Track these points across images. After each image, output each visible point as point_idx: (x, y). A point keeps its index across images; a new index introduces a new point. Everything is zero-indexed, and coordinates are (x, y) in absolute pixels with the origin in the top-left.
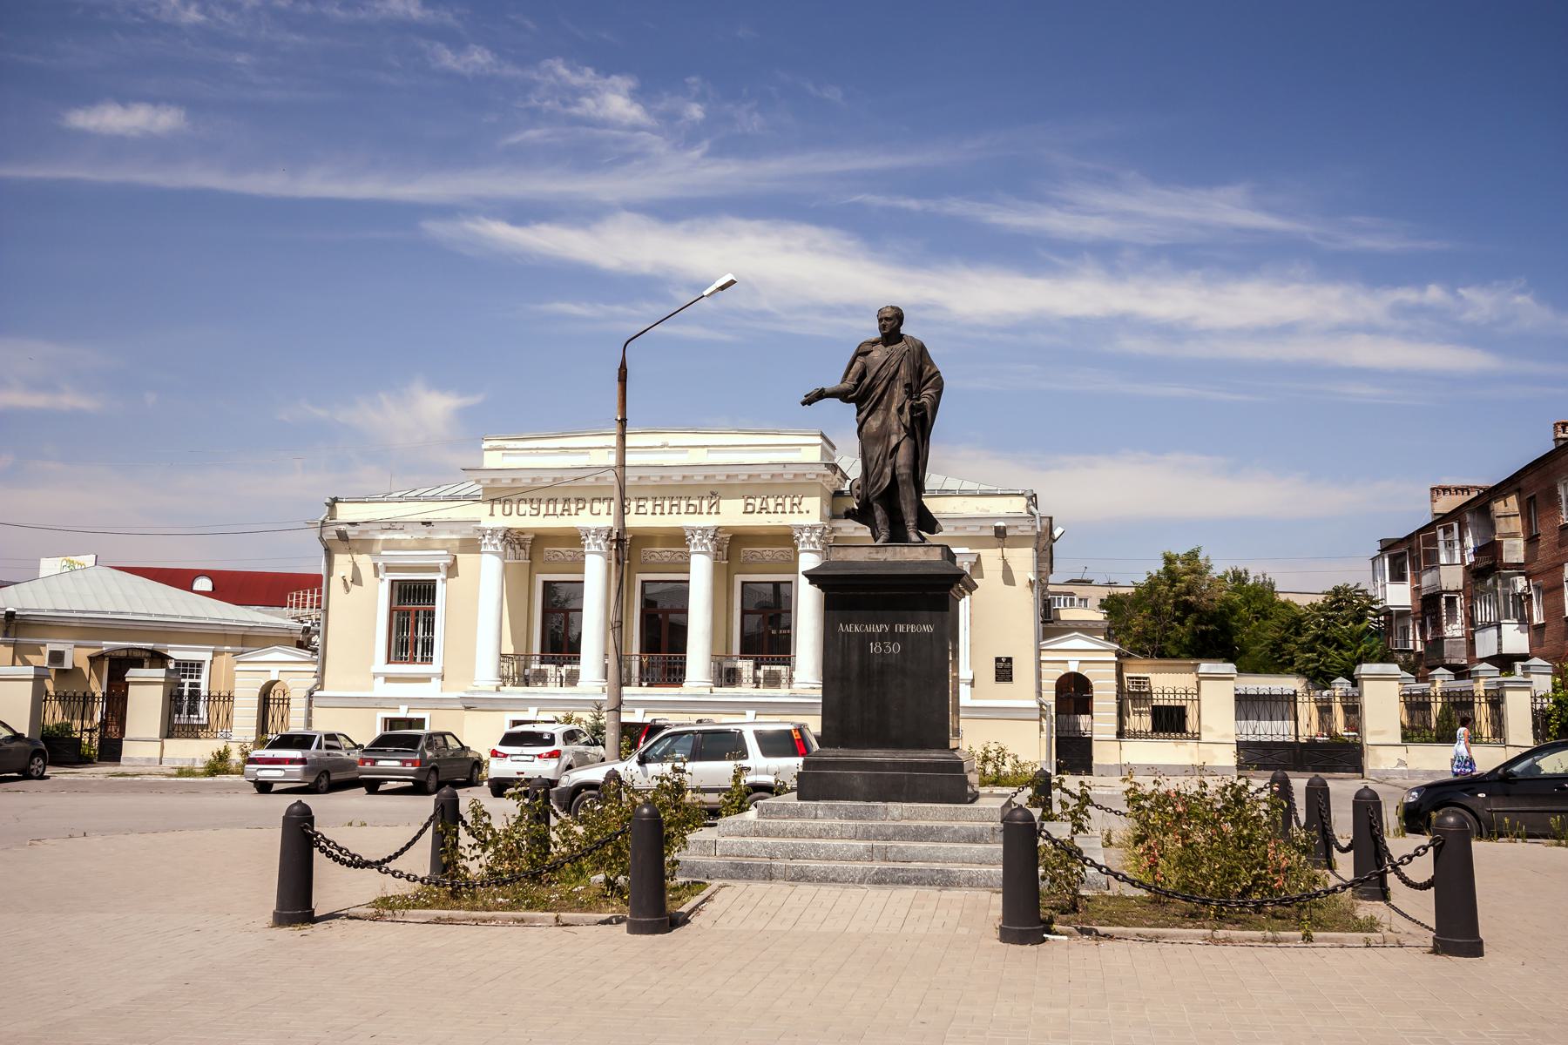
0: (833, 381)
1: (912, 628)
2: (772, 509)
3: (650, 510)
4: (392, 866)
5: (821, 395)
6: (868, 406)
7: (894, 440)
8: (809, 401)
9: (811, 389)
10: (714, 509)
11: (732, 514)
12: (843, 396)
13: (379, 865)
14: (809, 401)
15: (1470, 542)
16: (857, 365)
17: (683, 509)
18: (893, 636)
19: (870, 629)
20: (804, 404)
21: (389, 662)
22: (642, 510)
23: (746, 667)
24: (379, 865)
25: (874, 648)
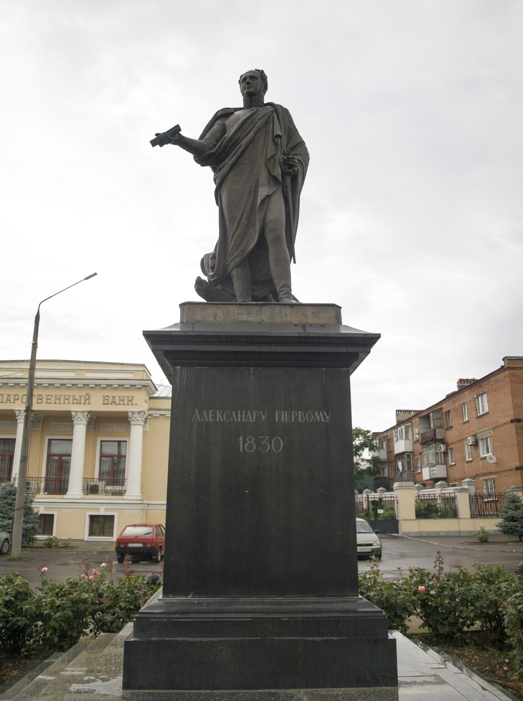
1: (300, 416)
2: (117, 402)
3: (53, 402)
5: (172, 137)
6: (230, 161)
7: (263, 192)
8: (160, 140)
9: (164, 129)
10: (87, 402)
11: (97, 404)
14: (160, 140)
15: (416, 430)
16: (216, 127)
17: (71, 402)
19: (239, 417)
20: (154, 143)
22: (49, 401)
23: (101, 485)
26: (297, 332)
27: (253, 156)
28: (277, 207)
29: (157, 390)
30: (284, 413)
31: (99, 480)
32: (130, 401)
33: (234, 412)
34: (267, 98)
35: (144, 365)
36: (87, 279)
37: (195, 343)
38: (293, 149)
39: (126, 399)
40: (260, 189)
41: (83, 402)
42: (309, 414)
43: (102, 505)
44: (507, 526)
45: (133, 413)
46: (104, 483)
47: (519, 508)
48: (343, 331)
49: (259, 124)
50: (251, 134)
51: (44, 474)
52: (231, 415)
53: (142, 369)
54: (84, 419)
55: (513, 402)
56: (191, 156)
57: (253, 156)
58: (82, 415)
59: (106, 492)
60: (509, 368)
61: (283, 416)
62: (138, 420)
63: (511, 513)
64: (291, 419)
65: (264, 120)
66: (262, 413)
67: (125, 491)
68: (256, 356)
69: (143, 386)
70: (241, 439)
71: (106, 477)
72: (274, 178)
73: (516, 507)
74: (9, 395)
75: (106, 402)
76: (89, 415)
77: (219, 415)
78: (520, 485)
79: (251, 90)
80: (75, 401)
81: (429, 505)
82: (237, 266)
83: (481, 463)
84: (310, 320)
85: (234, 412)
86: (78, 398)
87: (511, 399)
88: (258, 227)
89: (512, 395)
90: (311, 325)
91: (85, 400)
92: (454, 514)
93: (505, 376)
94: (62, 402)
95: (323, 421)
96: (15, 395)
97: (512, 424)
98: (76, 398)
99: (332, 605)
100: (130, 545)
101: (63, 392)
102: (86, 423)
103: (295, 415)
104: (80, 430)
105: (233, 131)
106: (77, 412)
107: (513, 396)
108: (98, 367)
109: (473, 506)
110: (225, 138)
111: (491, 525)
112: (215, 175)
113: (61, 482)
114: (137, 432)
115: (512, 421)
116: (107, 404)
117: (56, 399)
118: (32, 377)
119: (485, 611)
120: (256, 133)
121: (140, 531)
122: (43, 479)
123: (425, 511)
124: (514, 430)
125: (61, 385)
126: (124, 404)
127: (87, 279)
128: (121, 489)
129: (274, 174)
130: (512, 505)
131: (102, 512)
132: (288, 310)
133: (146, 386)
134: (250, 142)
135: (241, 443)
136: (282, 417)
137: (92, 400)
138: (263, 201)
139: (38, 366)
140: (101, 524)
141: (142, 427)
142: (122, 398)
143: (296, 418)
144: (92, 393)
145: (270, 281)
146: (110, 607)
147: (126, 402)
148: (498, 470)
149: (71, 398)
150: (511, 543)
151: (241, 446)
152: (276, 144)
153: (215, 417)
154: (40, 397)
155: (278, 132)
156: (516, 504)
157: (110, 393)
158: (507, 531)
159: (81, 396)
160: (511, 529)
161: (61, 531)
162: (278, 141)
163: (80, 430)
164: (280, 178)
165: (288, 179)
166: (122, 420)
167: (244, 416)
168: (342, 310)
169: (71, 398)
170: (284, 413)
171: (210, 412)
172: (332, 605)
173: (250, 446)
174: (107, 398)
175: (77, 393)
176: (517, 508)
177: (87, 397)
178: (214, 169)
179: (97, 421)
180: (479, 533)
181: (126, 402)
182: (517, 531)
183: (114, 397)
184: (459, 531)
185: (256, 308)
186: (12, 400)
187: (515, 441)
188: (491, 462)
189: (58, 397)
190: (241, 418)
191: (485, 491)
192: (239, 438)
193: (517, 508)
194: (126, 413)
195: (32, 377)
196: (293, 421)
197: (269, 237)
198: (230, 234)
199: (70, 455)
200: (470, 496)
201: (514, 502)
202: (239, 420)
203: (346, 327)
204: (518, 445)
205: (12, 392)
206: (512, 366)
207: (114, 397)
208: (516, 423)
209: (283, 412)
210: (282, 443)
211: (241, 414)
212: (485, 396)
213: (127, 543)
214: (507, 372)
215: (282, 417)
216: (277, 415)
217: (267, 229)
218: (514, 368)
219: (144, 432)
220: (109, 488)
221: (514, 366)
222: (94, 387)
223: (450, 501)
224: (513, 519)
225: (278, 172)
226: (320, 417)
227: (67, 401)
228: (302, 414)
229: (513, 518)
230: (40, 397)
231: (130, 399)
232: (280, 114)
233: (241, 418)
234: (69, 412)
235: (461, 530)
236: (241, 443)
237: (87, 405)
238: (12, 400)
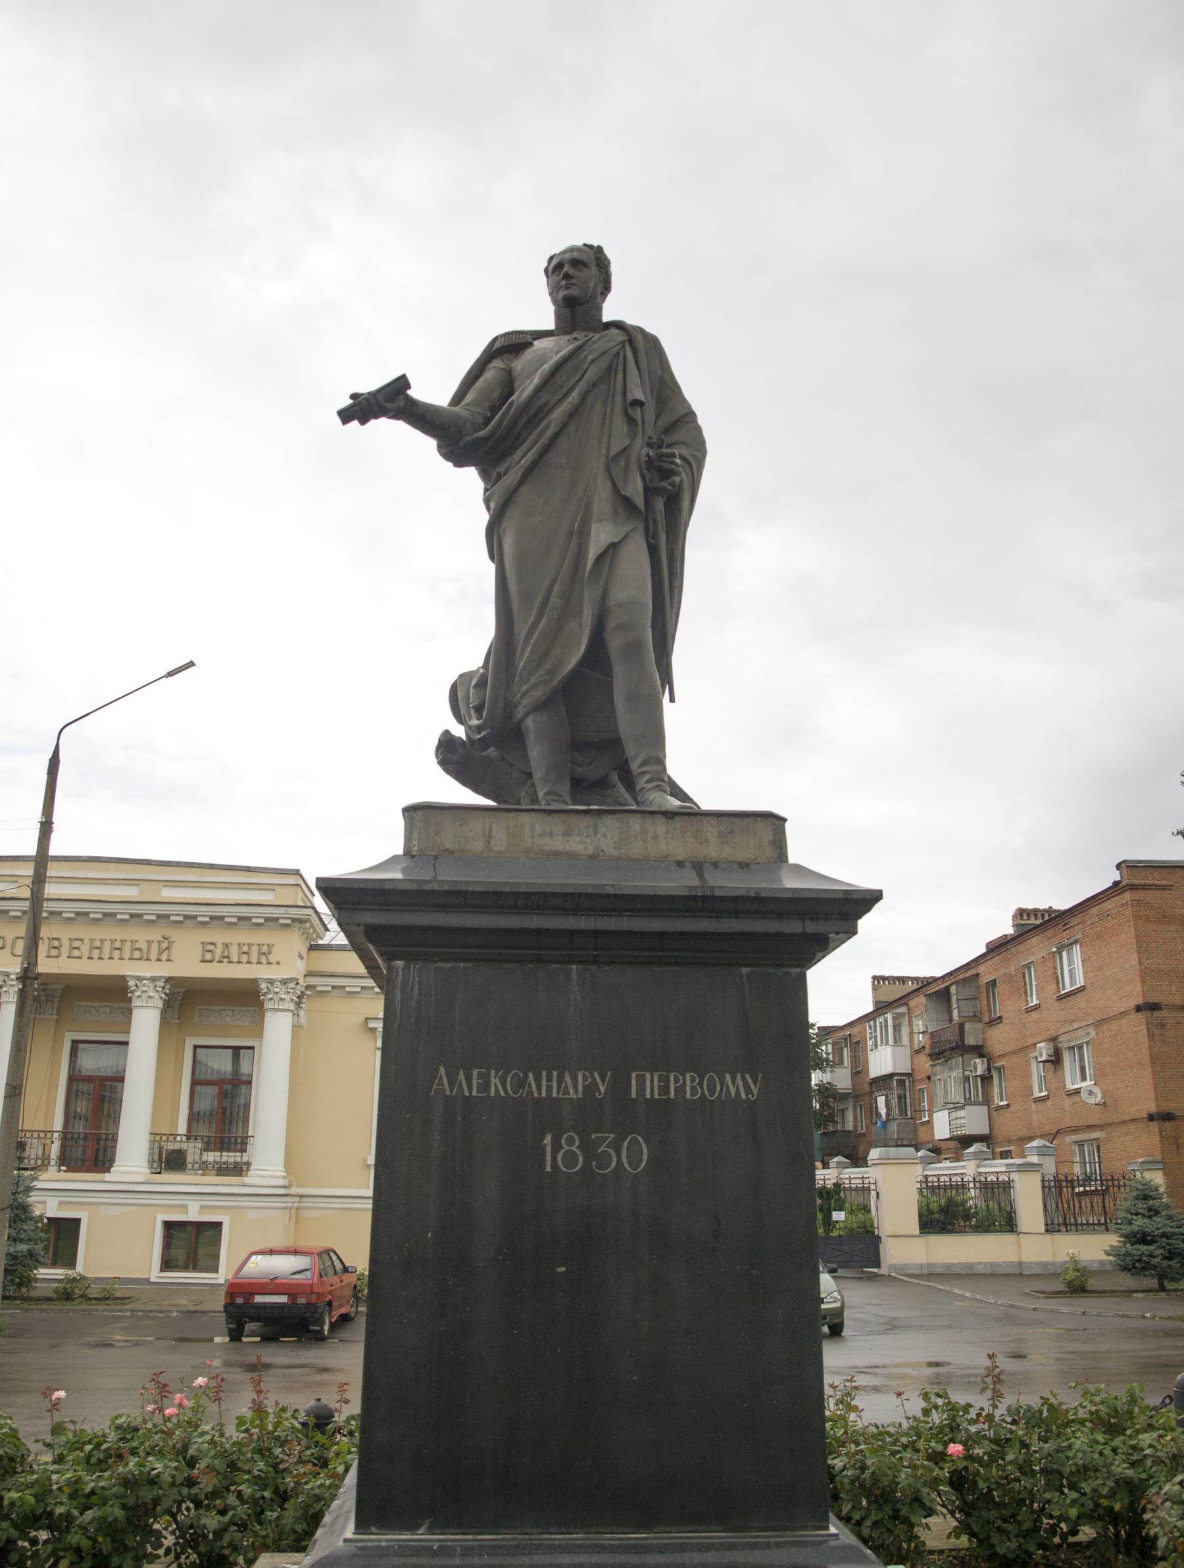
1: (689, 1085)
2: (235, 958)
3: (86, 955)
5: (390, 401)
6: (522, 458)
7: (601, 535)
8: (361, 409)
9: (370, 384)
10: (164, 956)
11: (188, 962)
14: (361, 409)
15: (919, 1025)
16: (489, 375)
17: (127, 955)
18: (624, 1114)
19: (543, 1087)
20: (346, 416)
22: (76, 953)
23: (193, 1150)
25: (560, 1154)
26: (680, 883)
27: (576, 441)
29: (327, 930)
30: (652, 1077)
31: (188, 1138)
32: (265, 954)
33: (531, 1075)
34: (611, 310)
35: (297, 873)
36: (170, 674)
37: (441, 908)
38: (667, 431)
39: (255, 949)
40: (595, 529)
41: (154, 955)
42: (711, 1079)
43: (193, 1196)
44: (1131, 1255)
45: (271, 982)
46: (199, 1145)
47: (1157, 1213)
48: (791, 883)
49: (593, 372)
50: (574, 396)
51: (58, 1125)
52: (521, 1083)
53: (292, 880)
54: (157, 996)
55: (1140, 964)
56: (429, 444)
57: (576, 441)
58: (152, 985)
59: (204, 1167)
60: (1132, 887)
61: (648, 1084)
62: (282, 999)
63: (1139, 1223)
64: (667, 1092)
65: (603, 363)
66: (597, 1078)
67: (248, 1164)
68: (585, 946)
69: (294, 920)
70: (548, 1140)
71: (203, 1130)
72: (628, 502)
73: (1150, 1209)
75: (208, 956)
76: (168, 986)
77: (495, 1081)
78: (1158, 1157)
79: (574, 292)
80: (137, 954)
81: (950, 1201)
82: (538, 708)
83: (1067, 1102)
84: (713, 850)
85: (531, 1075)
86: (144, 946)
87: (1135, 957)
88: (588, 618)
89: (1139, 948)
90: (715, 864)
91: (160, 952)
92: (1008, 1224)
93: (1123, 905)
94: (106, 954)
95: (743, 1096)
97: (1139, 1015)
98: (138, 945)
100: (259, 1299)
101: (107, 933)
102: (160, 1004)
103: (676, 1081)
104: (146, 1022)
105: (530, 389)
106: (140, 979)
108: (191, 876)
110: (512, 403)
111: (1094, 1248)
112: (486, 490)
113: (98, 1140)
114: (278, 1028)
115: (1138, 1009)
116: (211, 961)
117: (92, 948)
118: (37, 898)
119: (1104, 1502)
120: (584, 396)
121: (284, 1265)
122: (56, 1135)
123: (942, 1215)
124: (1143, 1027)
125: (105, 915)
126: (249, 963)
127: (170, 674)
128: (238, 1160)
129: (628, 491)
130: (1141, 1206)
131: (194, 1213)
133: (301, 921)
134: (572, 415)
135: (549, 1150)
136: (647, 1085)
137: (176, 953)
138: (600, 558)
139: (53, 871)
140: (190, 1242)
141: (290, 1014)
142: (245, 949)
143: (680, 1090)
144: (175, 935)
145: (613, 744)
146: (214, 1494)
147: (254, 959)
148: (1108, 1120)
149: (128, 945)
150: (1141, 1295)
151: (549, 1158)
152: (631, 421)
153: (485, 1087)
154: (56, 943)
155: (637, 393)
156: (1151, 1202)
157: (219, 937)
158: (1130, 1265)
159: (149, 943)
160: (1140, 1261)
161: (96, 1259)
162: (637, 413)
163: (146, 1022)
164: (640, 502)
165: (659, 504)
166: (246, 998)
167: (555, 1084)
168: (787, 825)
169: (128, 945)
170: (652, 1077)
171: (475, 1072)
173: (570, 1158)
174: (210, 947)
175: (142, 936)
176: (1153, 1212)
177: (165, 945)
178: (485, 475)
179: (186, 1001)
181: (254, 959)
182: (1154, 1267)
183: (226, 946)
184: (1020, 1263)
185: (586, 821)
187: (1145, 1055)
188: (1092, 1101)
189: (97, 944)
190: (549, 1088)
191: (1077, 1169)
192: (543, 1139)
193: (1153, 1212)
194: (255, 981)
195: (37, 898)
196: (672, 1096)
197: (615, 643)
198: (521, 631)
199: (121, 1080)
200: (1043, 1181)
201: (1146, 1197)
202: (544, 1094)
203: (799, 870)
204: (1153, 1064)
206: (1137, 882)
207: (226, 946)
208: (1149, 1013)
209: (648, 1076)
210: (645, 1151)
211: (549, 1079)
212: (1077, 949)
213: (252, 1294)
214: (1127, 896)
215: (647, 1085)
216: (634, 1082)
217: (611, 625)
218: (1144, 887)
219: (296, 1027)
220: (211, 1157)
221: (1142, 882)
222: (181, 922)
223: (999, 1190)
224: (1143, 1238)
225: (635, 488)
227: (116, 954)
228: (693, 1080)
229: (1145, 1235)
230: (56, 943)
231: (265, 949)
232: (640, 348)
233: (549, 1088)
234: (123, 979)
235: (1023, 1260)
236: (549, 1150)
237: (164, 964)
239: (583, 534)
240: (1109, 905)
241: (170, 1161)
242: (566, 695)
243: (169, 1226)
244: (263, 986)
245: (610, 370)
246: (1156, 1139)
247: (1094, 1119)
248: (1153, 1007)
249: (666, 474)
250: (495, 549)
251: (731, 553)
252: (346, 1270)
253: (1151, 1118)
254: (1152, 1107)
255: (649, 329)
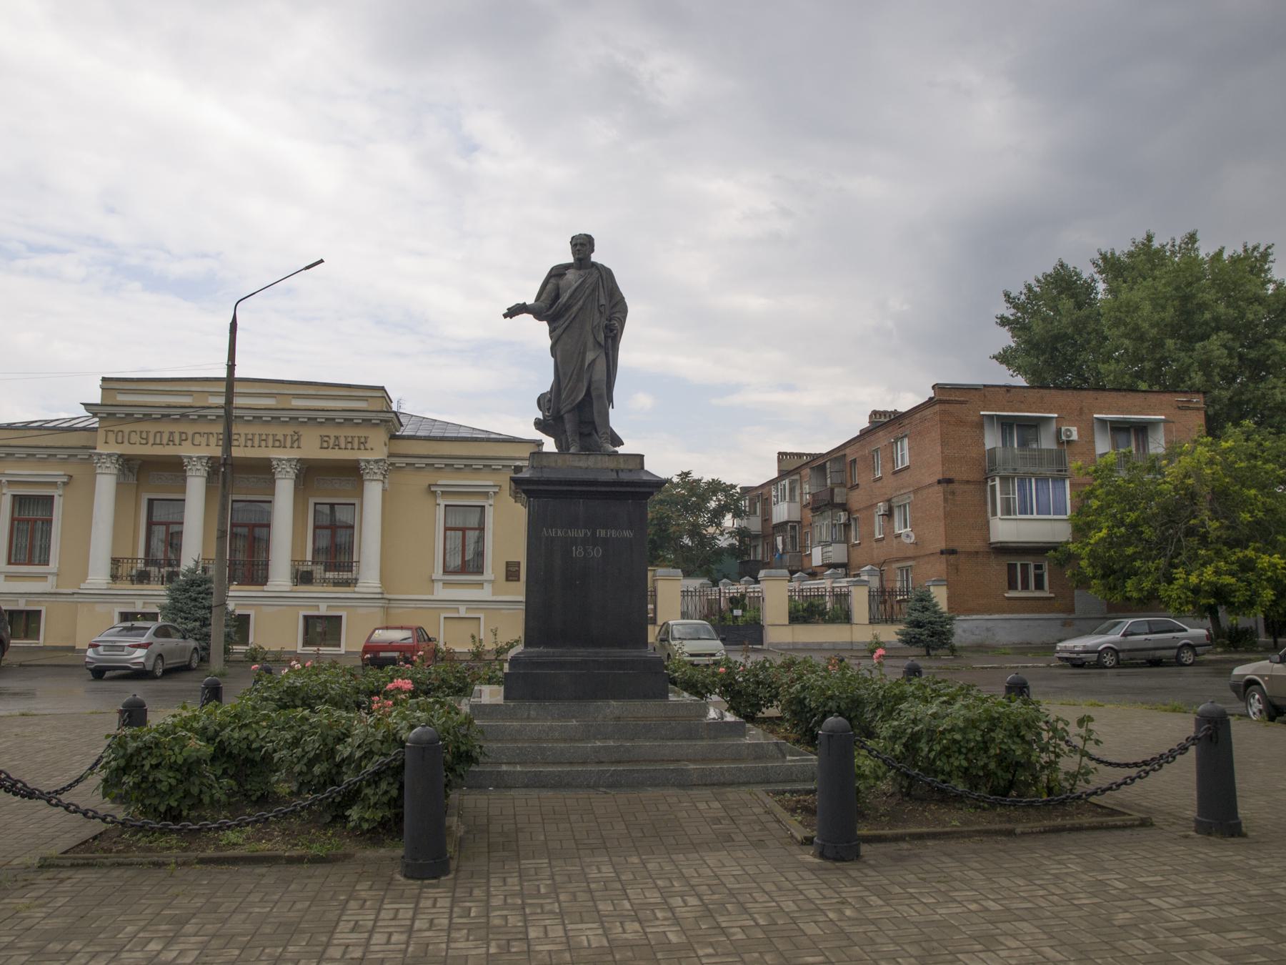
0: (530, 300)
1: (613, 533)
4: (65, 798)
7: (590, 356)
10: (296, 445)
11: (311, 448)
12: (537, 311)
13: (51, 798)
15: (807, 488)
16: (549, 286)
17: (270, 444)
19: (572, 533)
20: (505, 316)
21: (9, 563)
23: (318, 571)
24: (51, 798)
25: (577, 552)
26: (613, 476)
27: (581, 306)
28: (601, 366)
32: (363, 443)
34: (595, 258)
35: (382, 389)
39: (356, 440)
41: (288, 444)
43: (322, 598)
45: (368, 461)
47: (928, 609)
48: (645, 478)
50: (581, 303)
53: (379, 394)
56: (531, 316)
57: (581, 306)
59: (325, 581)
60: (941, 402)
63: (916, 614)
67: (357, 580)
71: (322, 558)
72: (599, 344)
74: (171, 433)
75: (325, 445)
78: (944, 577)
80: (277, 444)
81: (811, 605)
82: (569, 412)
86: (282, 438)
88: (585, 384)
91: (293, 443)
92: (843, 616)
94: (256, 443)
96: (181, 433)
99: (631, 653)
100: (382, 654)
104: (284, 490)
106: (280, 460)
107: (944, 443)
108: (311, 391)
109: (874, 607)
111: (890, 634)
112: (551, 332)
114: (373, 492)
115: (939, 482)
117: (246, 440)
121: (396, 636)
130: (918, 605)
131: (323, 610)
132: (607, 458)
133: (386, 421)
134: (581, 309)
136: (602, 533)
137: (303, 442)
140: (322, 629)
144: (304, 431)
145: (592, 423)
146: (439, 687)
155: (603, 301)
157: (332, 432)
158: (910, 640)
159: (285, 436)
161: (260, 637)
163: (284, 490)
166: (352, 472)
169: (271, 438)
172: (631, 653)
175: (280, 432)
179: (309, 473)
180: (871, 643)
183: (337, 438)
184: (852, 643)
186: (177, 442)
187: (941, 513)
188: (908, 541)
193: (925, 609)
194: (358, 461)
197: (594, 394)
199: (268, 526)
201: (922, 600)
204: (945, 518)
205: (177, 428)
207: (337, 438)
212: (906, 441)
214: (937, 407)
215: (602, 533)
219: (384, 490)
220: (330, 575)
223: (842, 598)
224: (918, 624)
225: (601, 338)
226: (627, 534)
227: (263, 444)
232: (605, 276)
234: (269, 460)
237: (295, 450)
238: (177, 442)
239: (584, 353)
240: (928, 412)
241: (303, 578)
242: (578, 403)
243: (306, 618)
244: (362, 464)
245: (593, 290)
246: (944, 566)
247: (910, 554)
248: (949, 481)
249: (612, 331)
250: (553, 353)
251: (635, 351)
252: (430, 640)
253: (942, 553)
254: (943, 546)
255: (606, 265)
